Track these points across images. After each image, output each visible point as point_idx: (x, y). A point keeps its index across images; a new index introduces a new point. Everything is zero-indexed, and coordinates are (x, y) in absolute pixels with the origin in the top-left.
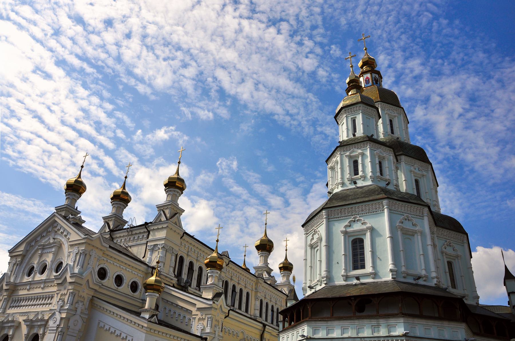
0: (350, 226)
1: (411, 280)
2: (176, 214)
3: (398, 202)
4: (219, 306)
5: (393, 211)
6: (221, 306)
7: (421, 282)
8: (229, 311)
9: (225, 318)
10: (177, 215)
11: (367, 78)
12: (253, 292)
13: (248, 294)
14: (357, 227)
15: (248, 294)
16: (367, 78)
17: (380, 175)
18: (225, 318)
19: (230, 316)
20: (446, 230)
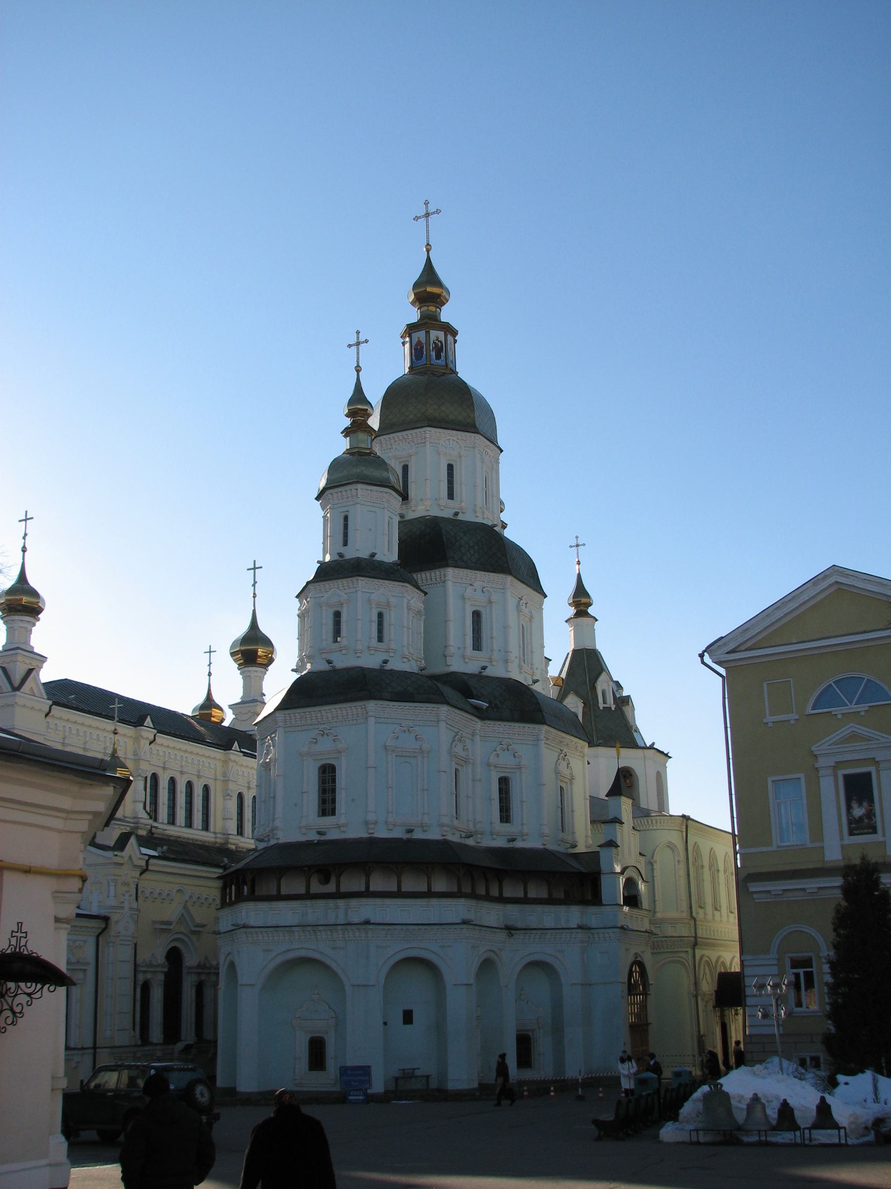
0: (316, 743)
1: (398, 833)
2: (30, 671)
3: (392, 703)
4: (126, 859)
5: (381, 720)
6: (130, 857)
7: (418, 835)
8: (147, 862)
9: (141, 874)
10: (34, 672)
11: (419, 343)
12: (219, 784)
13: (206, 789)
14: (325, 745)
15: (206, 789)
16: (419, 343)
17: (374, 642)
18: (141, 874)
19: (150, 868)
20: (502, 724)
